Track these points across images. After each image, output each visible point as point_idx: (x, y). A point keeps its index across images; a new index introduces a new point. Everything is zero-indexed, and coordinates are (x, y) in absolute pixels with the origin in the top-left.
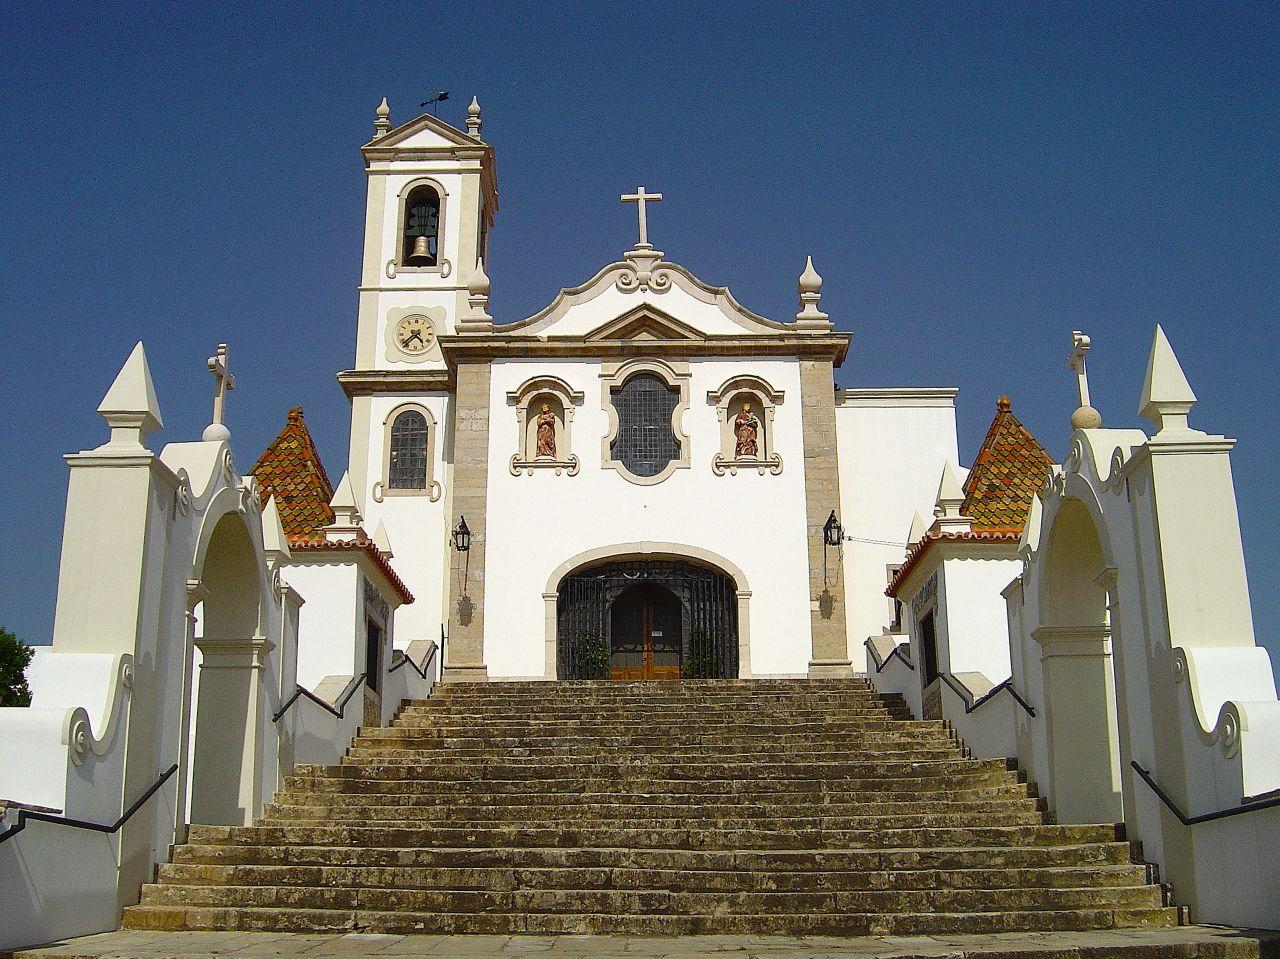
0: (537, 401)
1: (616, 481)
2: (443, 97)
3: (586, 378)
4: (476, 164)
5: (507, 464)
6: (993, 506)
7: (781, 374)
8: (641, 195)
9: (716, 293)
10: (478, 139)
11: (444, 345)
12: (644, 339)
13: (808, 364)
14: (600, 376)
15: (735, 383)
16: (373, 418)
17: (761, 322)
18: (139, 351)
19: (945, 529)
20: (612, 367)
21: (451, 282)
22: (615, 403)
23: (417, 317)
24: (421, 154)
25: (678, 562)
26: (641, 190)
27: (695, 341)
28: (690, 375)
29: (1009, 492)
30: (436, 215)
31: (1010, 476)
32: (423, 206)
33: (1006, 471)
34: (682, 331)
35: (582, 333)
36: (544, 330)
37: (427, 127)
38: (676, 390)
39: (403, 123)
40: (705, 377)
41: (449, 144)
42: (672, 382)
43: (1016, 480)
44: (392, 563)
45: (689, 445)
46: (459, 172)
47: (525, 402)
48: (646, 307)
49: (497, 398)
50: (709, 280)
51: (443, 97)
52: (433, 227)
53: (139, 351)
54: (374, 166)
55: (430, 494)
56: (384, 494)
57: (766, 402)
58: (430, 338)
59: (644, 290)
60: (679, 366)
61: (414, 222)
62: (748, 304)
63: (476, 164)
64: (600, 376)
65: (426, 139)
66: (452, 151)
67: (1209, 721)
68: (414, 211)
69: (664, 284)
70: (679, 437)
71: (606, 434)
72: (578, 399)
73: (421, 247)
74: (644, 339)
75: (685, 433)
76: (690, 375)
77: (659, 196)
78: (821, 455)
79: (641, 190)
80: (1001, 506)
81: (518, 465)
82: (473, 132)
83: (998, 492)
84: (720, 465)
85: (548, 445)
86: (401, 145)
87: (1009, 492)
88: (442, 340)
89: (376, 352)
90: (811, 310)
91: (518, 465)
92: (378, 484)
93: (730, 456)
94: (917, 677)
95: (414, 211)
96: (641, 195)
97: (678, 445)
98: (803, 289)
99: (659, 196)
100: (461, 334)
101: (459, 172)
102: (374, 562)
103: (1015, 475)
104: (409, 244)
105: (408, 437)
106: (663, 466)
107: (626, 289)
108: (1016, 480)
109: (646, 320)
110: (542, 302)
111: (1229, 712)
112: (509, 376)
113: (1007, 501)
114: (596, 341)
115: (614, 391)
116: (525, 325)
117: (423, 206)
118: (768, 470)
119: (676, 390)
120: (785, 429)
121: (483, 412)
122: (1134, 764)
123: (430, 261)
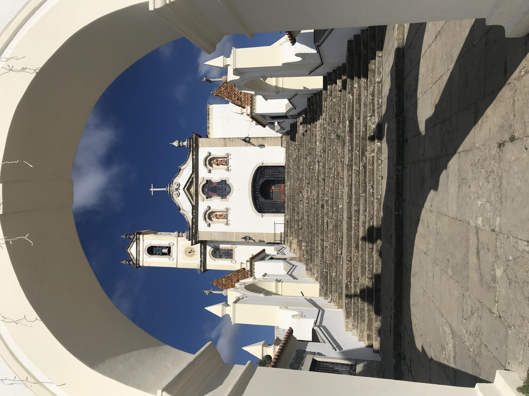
0: (210, 219)
1: (231, 197)
3: (203, 206)
4: (141, 236)
6: (243, 99)
7: (203, 153)
10: (134, 236)
11: (194, 244)
12: (193, 190)
13: (200, 145)
14: (203, 201)
16: (213, 264)
17: (189, 157)
18: (207, 308)
19: (249, 113)
20: (200, 198)
21: (175, 243)
22: (211, 197)
24: (138, 252)
25: (254, 181)
26: (151, 189)
27: (194, 176)
28: (203, 177)
29: (239, 95)
30: (156, 247)
31: (235, 94)
32: (152, 250)
33: (234, 95)
34: (191, 179)
35: (191, 206)
36: (189, 217)
37: (130, 250)
38: (207, 181)
39: (128, 256)
40: (204, 174)
41: (135, 243)
42: (205, 182)
43: (236, 93)
44: (254, 255)
45: (222, 178)
46: (143, 241)
48: (184, 188)
49: (209, 229)
50: (177, 171)
52: (159, 248)
53: (207, 308)
55: (234, 248)
56: (234, 260)
57: (211, 157)
58: (191, 248)
59: (179, 189)
60: (200, 181)
62: (184, 161)
64: (203, 201)
67: (299, 59)
68: (154, 253)
69: (178, 184)
70: (220, 181)
71: (219, 200)
72: (209, 208)
73: (165, 251)
74: (193, 190)
75: (219, 179)
76: (203, 177)
77: (152, 185)
78: (226, 141)
80: (243, 97)
81: (227, 224)
82: (132, 237)
83: (239, 98)
84: (228, 170)
86: (135, 257)
87: (239, 95)
88: (192, 245)
89: (194, 263)
91: (227, 224)
92: (231, 262)
93: (226, 167)
94: (286, 120)
95: (154, 253)
97: (222, 181)
98: (179, 145)
99: (152, 185)
100: (191, 239)
101: (143, 241)
102: (253, 259)
103: (235, 93)
104: (164, 254)
105: (218, 253)
106: (228, 185)
107: (179, 195)
108: (236, 93)
109: (188, 187)
110: (182, 217)
111: (297, 55)
112: (202, 226)
113: (241, 95)
115: (207, 198)
116: (189, 223)
117: (152, 250)
118: (229, 157)
119: (207, 181)
120: (218, 152)
121: (213, 233)
122: (309, 74)
123: (169, 249)
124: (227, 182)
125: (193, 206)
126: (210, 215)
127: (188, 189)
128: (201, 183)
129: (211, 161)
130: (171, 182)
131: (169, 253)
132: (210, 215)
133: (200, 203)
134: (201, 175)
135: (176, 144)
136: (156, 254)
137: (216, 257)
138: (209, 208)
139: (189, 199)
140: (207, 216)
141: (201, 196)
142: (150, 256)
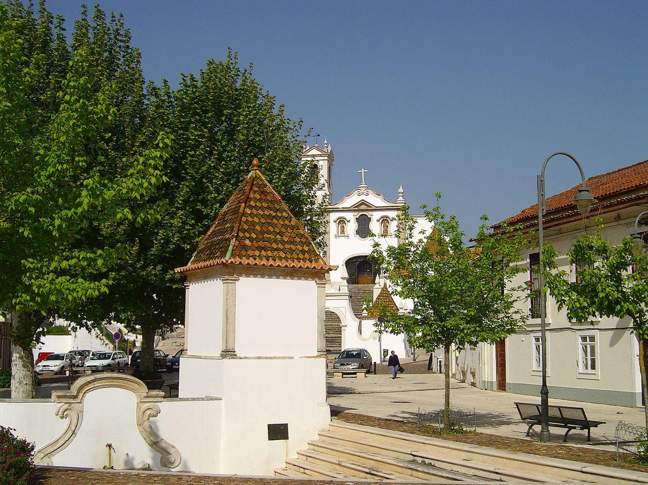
2: (319, 135)
4: (326, 158)
5: (334, 237)
7: (392, 214)
12: (363, 207)
15: (383, 217)
26: (363, 169)
47: (337, 222)
49: (332, 221)
51: (319, 135)
60: (371, 213)
63: (326, 158)
66: (321, 155)
72: (349, 221)
74: (363, 207)
79: (363, 169)
85: (343, 232)
90: (401, 198)
96: (363, 171)
109: (363, 203)
110: (341, 199)
112: (333, 216)
114: (352, 209)
115: (356, 219)
126: (342, 222)
127: (363, 204)
128: (368, 214)
129: (385, 221)
130: (368, 188)
132: (342, 222)
133: (352, 214)
134: (375, 213)
135: (401, 190)
138: (349, 221)
139: (355, 204)
140: (342, 219)
141: (358, 214)
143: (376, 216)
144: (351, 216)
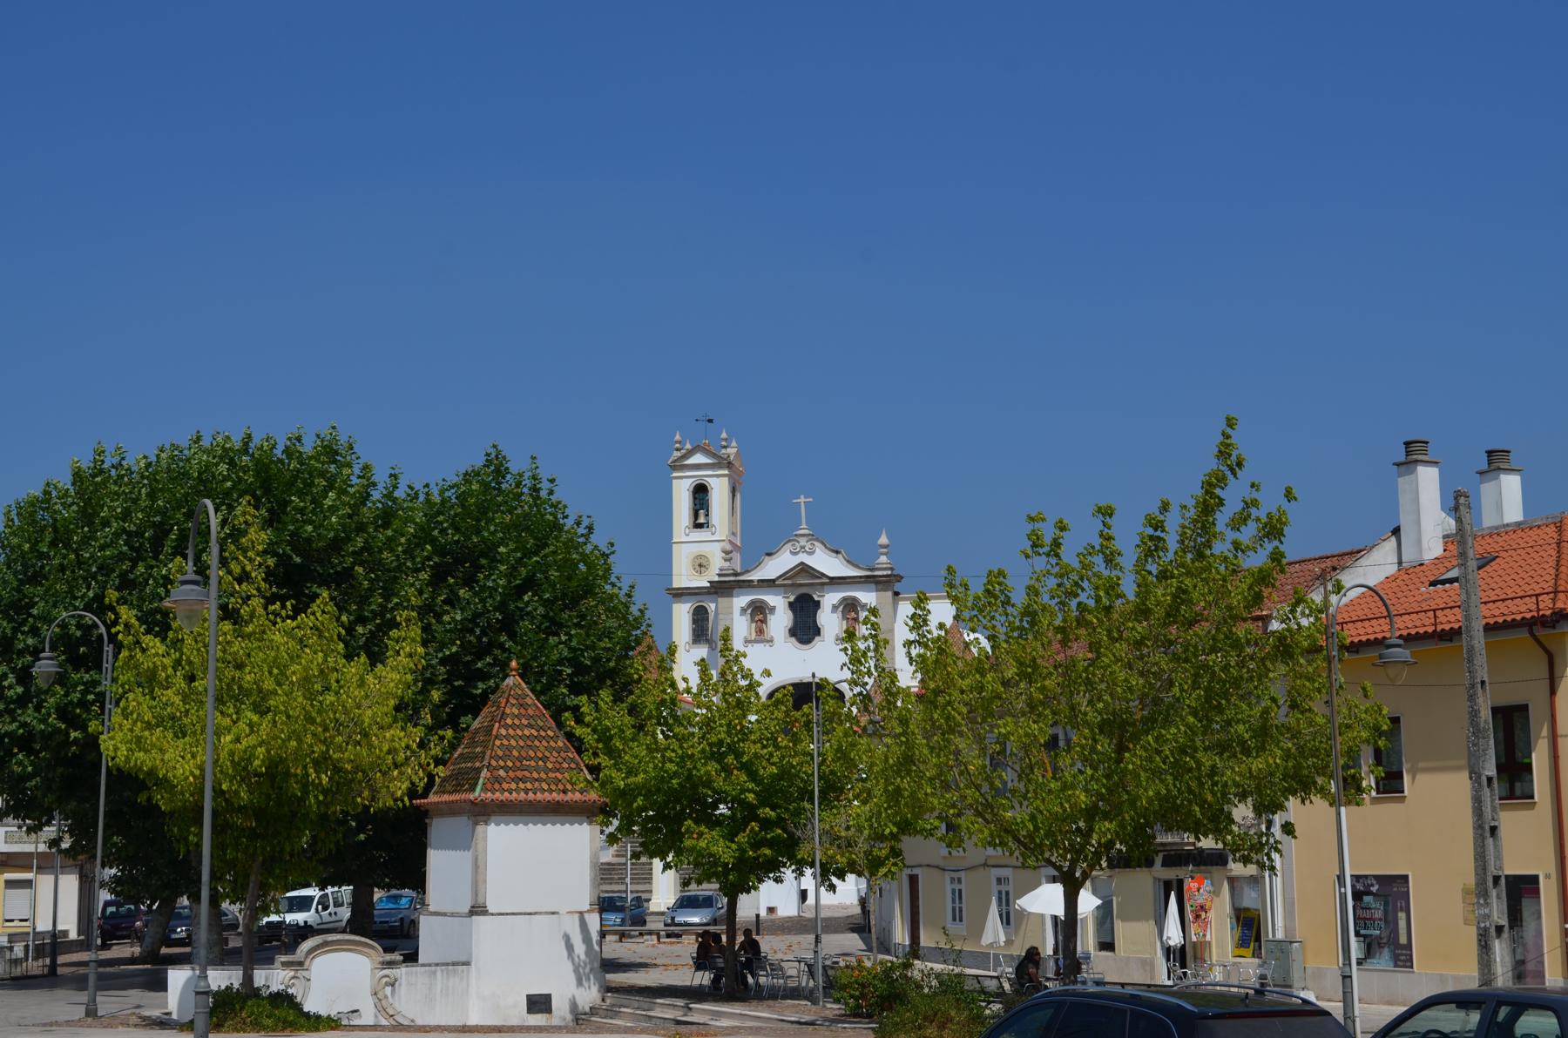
2: (710, 421)
5: (742, 641)
7: (867, 597)
8: (802, 500)
9: (837, 552)
23: (701, 556)
26: (802, 496)
32: (700, 492)
36: (755, 576)
38: (819, 602)
48: (802, 563)
54: (675, 475)
61: (697, 502)
65: (699, 458)
73: (702, 520)
79: (802, 496)
85: (760, 632)
86: (686, 463)
96: (802, 500)
104: (696, 516)
109: (804, 569)
112: (741, 600)
117: (700, 492)
124: (817, 638)
125: (773, 581)
126: (759, 612)
131: (698, 526)
132: (759, 612)
136: (695, 498)
137: (694, 614)
142: (692, 489)
143: (830, 599)
144: (779, 603)
